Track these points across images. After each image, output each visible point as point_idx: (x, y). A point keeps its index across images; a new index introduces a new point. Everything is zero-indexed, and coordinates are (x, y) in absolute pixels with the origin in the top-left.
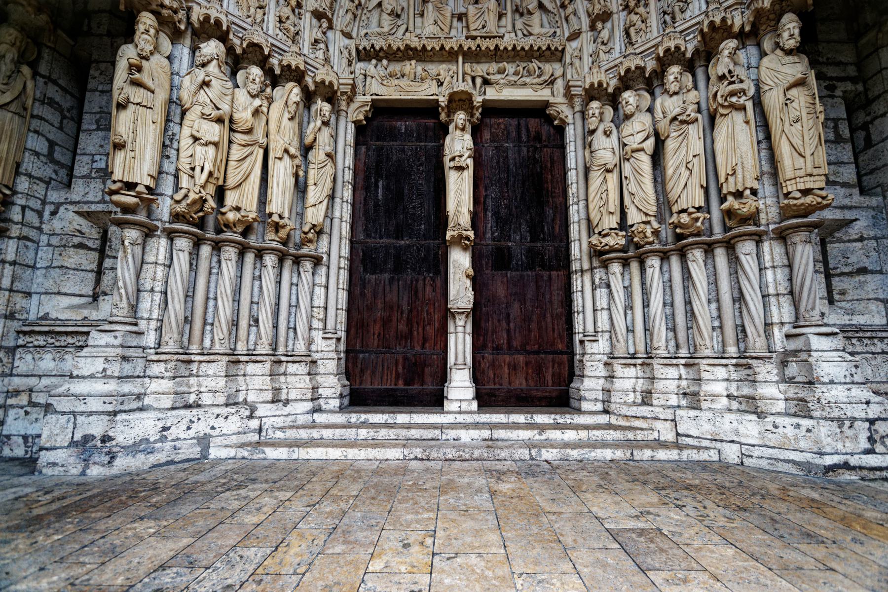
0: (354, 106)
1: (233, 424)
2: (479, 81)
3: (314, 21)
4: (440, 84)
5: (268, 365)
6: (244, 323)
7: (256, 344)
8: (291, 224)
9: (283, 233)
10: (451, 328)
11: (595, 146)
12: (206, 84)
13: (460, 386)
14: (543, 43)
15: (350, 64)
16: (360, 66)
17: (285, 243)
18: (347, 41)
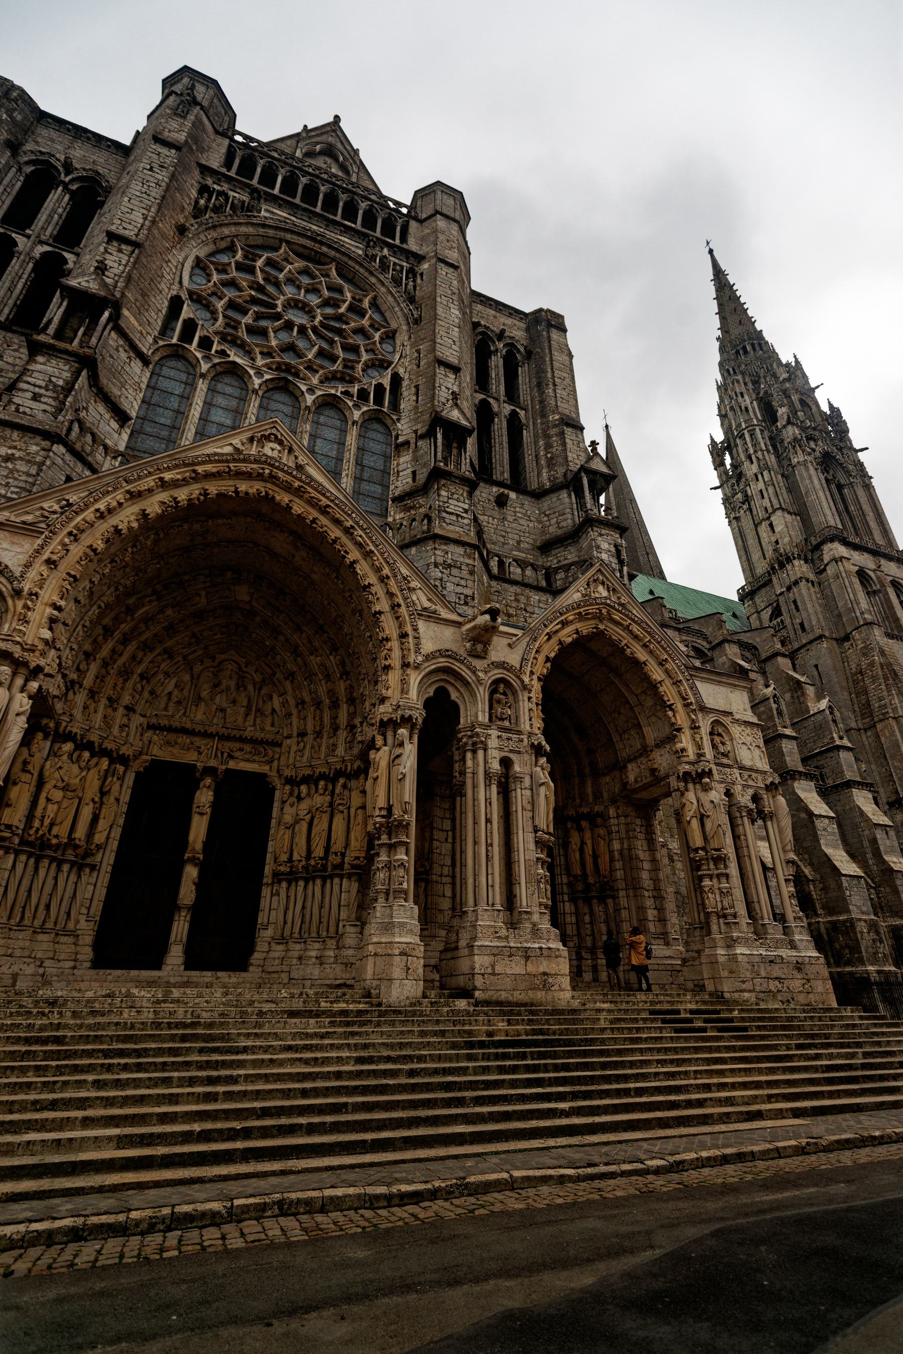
0: (138, 761)
1: (29, 970)
2: (225, 755)
3: (125, 712)
4: (200, 753)
5: (53, 935)
6: (42, 907)
7: (44, 922)
8: (82, 843)
9: (78, 851)
10: (176, 918)
11: (285, 810)
12: (60, 768)
13: (176, 955)
14: (270, 737)
15: (142, 735)
16: (148, 734)
17: (76, 857)
18: (142, 719)
